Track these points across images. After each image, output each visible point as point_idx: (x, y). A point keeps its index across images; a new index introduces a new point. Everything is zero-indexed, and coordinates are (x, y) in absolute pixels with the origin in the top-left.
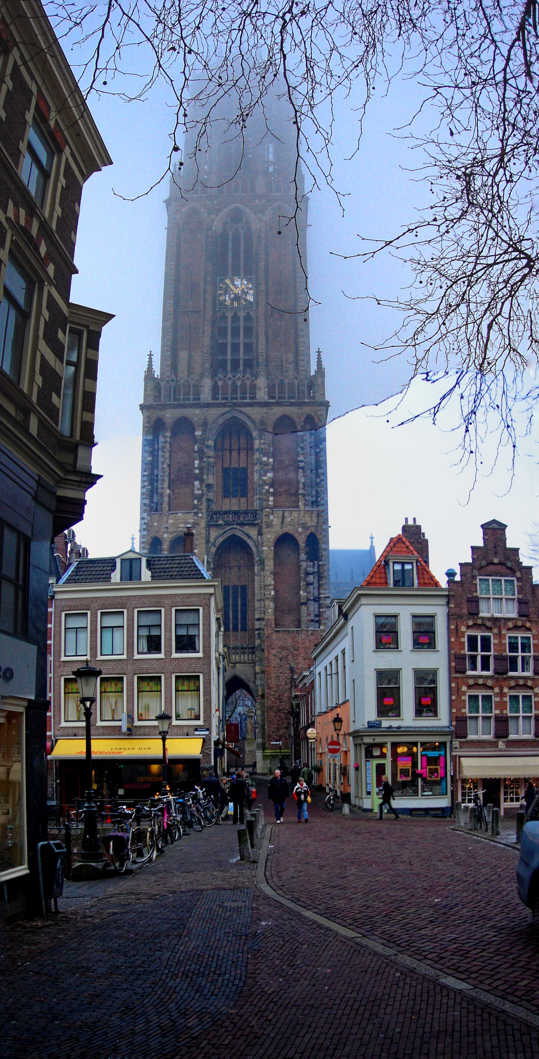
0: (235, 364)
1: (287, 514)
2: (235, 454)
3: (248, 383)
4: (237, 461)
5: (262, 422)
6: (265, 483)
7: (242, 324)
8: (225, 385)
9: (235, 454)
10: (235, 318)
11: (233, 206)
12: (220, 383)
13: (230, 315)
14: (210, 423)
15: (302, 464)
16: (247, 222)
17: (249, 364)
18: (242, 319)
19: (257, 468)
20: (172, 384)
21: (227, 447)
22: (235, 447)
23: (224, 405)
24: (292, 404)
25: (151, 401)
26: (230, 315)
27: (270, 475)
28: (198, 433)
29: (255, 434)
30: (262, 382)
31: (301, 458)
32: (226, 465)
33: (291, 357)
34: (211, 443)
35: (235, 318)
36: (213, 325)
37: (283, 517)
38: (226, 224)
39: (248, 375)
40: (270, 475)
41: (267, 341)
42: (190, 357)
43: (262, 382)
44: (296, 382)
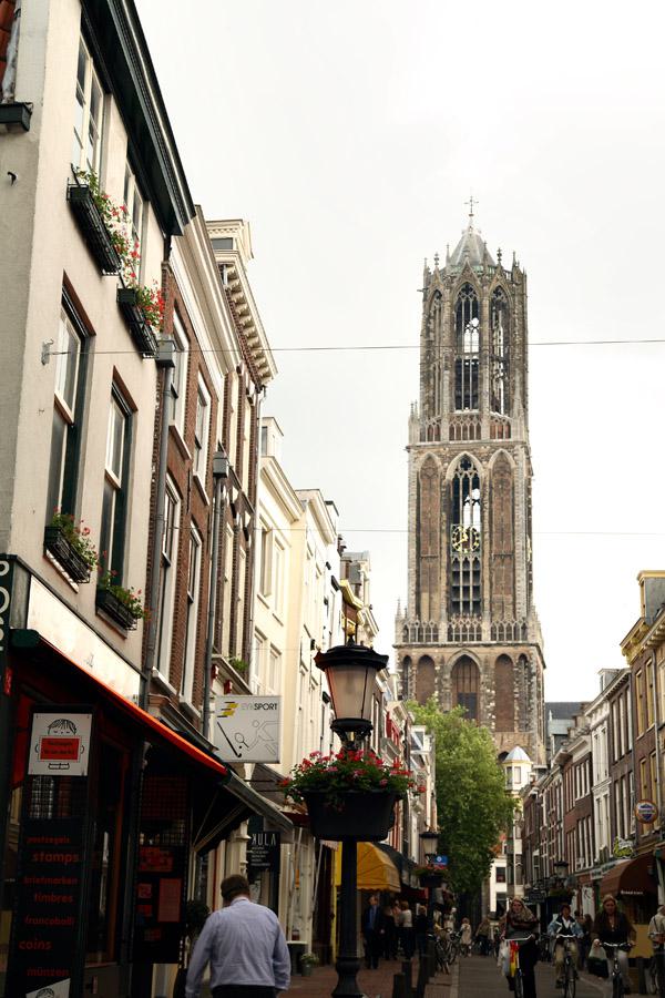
0: (466, 604)
1: (505, 737)
2: (467, 682)
3: (475, 626)
4: (466, 688)
5: (486, 661)
6: (488, 711)
7: (471, 569)
8: (457, 628)
9: (467, 682)
10: (466, 562)
11: (462, 454)
12: (454, 627)
13: (461, 560)
14: (446, 660)
15: (517, 695)
16: (475, 469)
17: (476, 604)
18: (471, 564)
19: (482, 698)
20: (417, 627)
21: (461, 675)
22: (467, 675)
23: (457, 646)
24: (509, 645)
25: (401, 642)
26: (461, 560)
27: (493, 704)
28: (437, 668)
29: (481, 669)
30: (486, 626)
31: (516, 690)
32: (460, 691)
33: (510, 598)
34: (447, 676)
35: (466, 562)
36: (447, 572)
37: (502, 739)
38: (457, 470)
39: (475, 620)
40: (493, 704)
41: (491, 587)
42: (431, 598)
43: (486, 626)
44: (513, 625)
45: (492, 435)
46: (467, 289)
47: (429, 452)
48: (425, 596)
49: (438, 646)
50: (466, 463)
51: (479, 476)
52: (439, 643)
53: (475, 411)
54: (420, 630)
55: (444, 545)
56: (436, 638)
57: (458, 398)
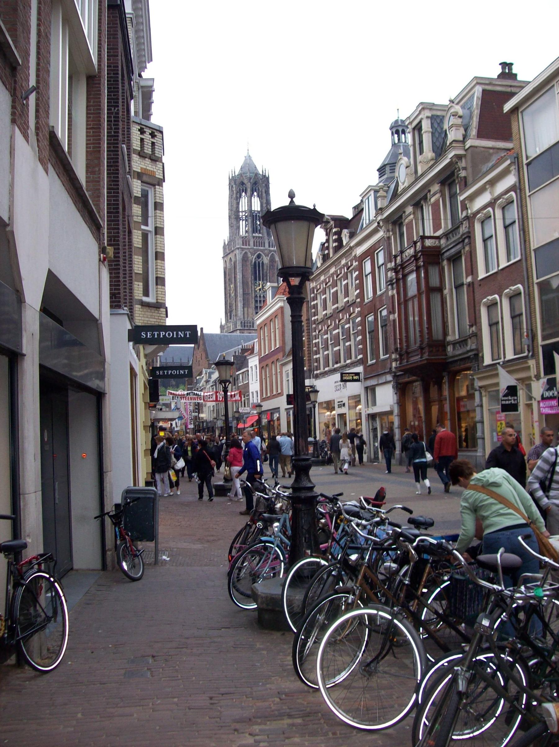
10: (260, 296)
13: (258, 296)
26: (258, 296)
45: (269, 246)
46: (255, 183)
47: (247, 251)
48: (246, 309)
49: (254, 330)
50: (259, 256)
51: (264, 262)
52: (254, 328)
53: (260, 235)
54: (244, 323)
55: (253, 289)
56: (253, 327)
57: (254, 230)
